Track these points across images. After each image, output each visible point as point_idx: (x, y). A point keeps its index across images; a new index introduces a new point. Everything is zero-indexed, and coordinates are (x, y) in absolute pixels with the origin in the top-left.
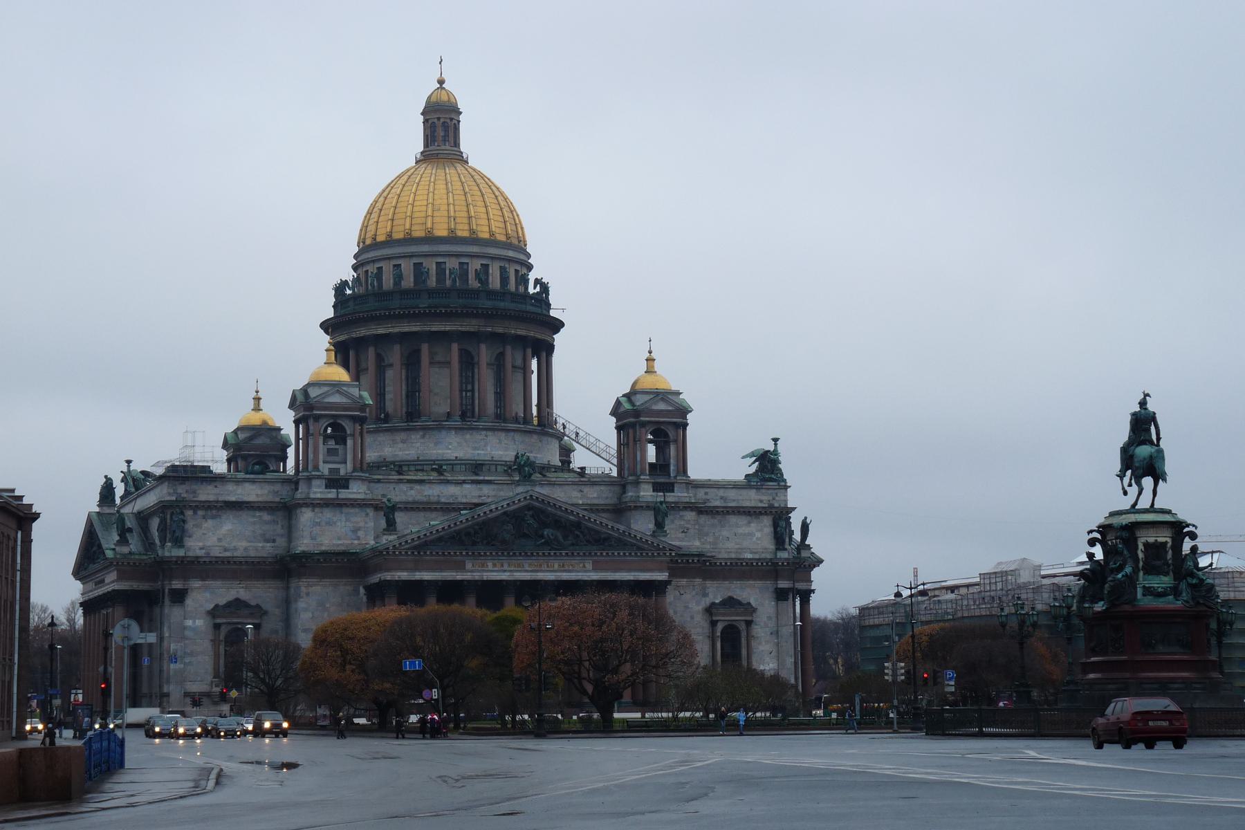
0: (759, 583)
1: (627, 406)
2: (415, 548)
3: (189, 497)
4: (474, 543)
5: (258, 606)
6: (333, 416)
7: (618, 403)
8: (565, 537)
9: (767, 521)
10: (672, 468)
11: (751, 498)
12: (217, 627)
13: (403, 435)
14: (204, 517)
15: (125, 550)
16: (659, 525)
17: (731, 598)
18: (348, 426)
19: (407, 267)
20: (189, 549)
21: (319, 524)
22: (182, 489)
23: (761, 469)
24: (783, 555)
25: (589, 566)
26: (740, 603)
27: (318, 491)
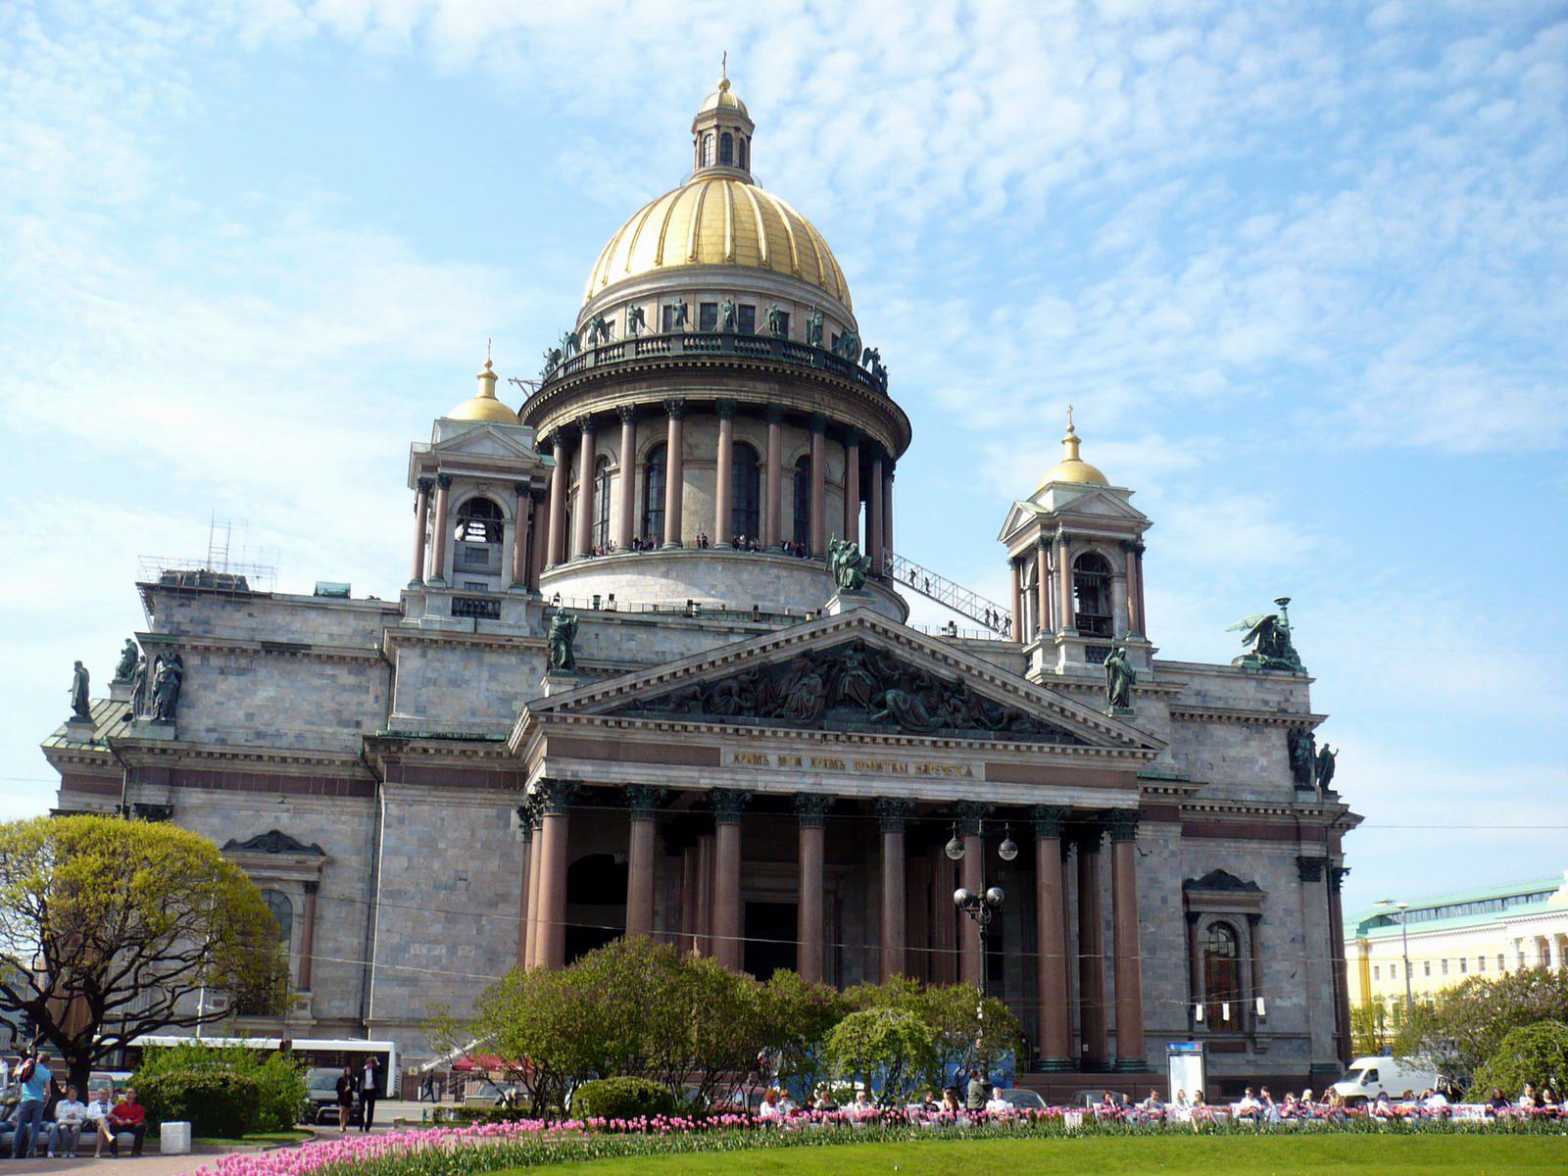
2: (611, 712)
3: (200, 630)
4: (739, 711)
5: (316, 850)
6: (479, 482)
8: (932, 710)
9: (1277, 739)
10: (1117, 624)
11: (1248, 696)
14: (222, 672)
15: (83, 734)
16: (1122, 701)
17: (1221, 873)
18: (510, 506)
19: (650, 311)
20: (185, 730)
21: (435, 683)
22: (182, 615)
25: (980, 772)
26: (1235, 884)
27: (433, 618)
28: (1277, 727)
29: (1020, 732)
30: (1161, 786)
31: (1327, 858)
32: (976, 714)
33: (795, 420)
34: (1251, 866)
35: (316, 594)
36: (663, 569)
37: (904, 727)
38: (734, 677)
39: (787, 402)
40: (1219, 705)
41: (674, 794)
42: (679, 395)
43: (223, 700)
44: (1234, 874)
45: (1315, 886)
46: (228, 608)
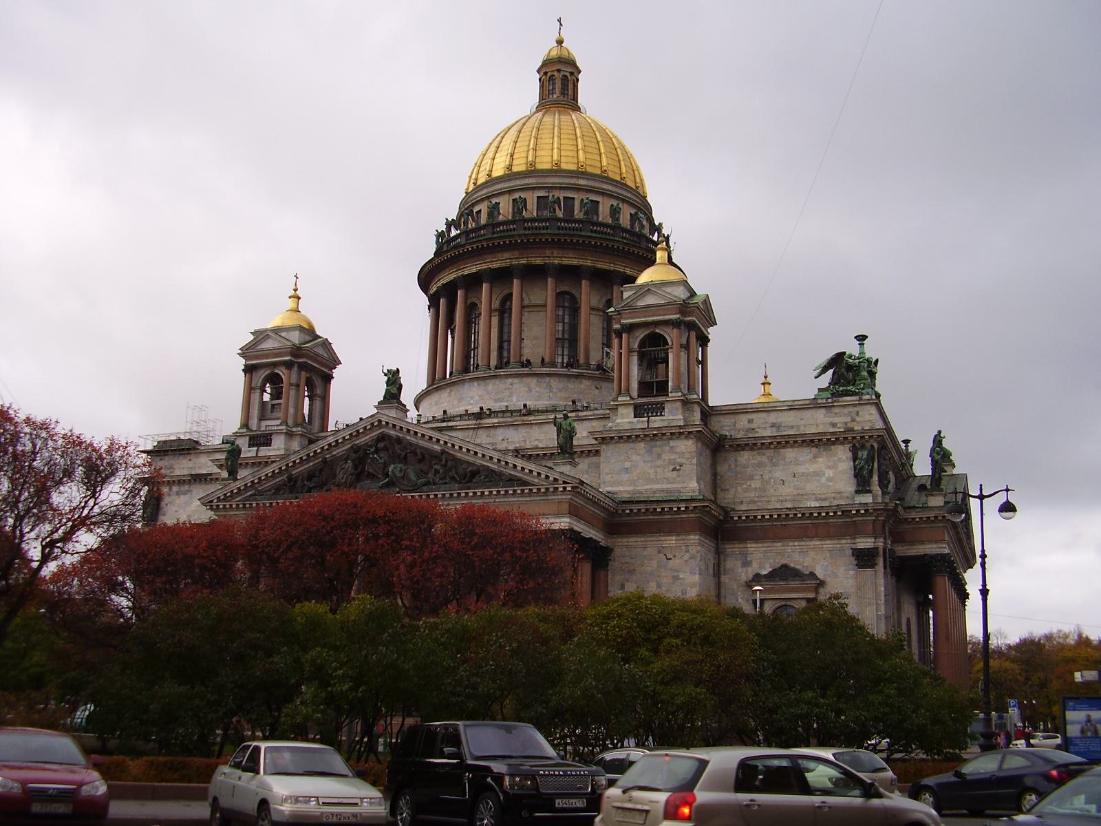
0: (828, 544)
9: (842, 455)
10: (670, 384)
11: (818, 422)
17: (785, 566)
23: (835, 381)
24: (867, 499)
28: (842, 443)
32: (453, 473)
34: (814, 559)
35: (223, 443)
36: (448, 391)
37: (400, 488)
39: (524, 261)
42: (460, 273)
43: (177, 509)
44: (798, 567)
45: (869, 571)
46: (181, 457)
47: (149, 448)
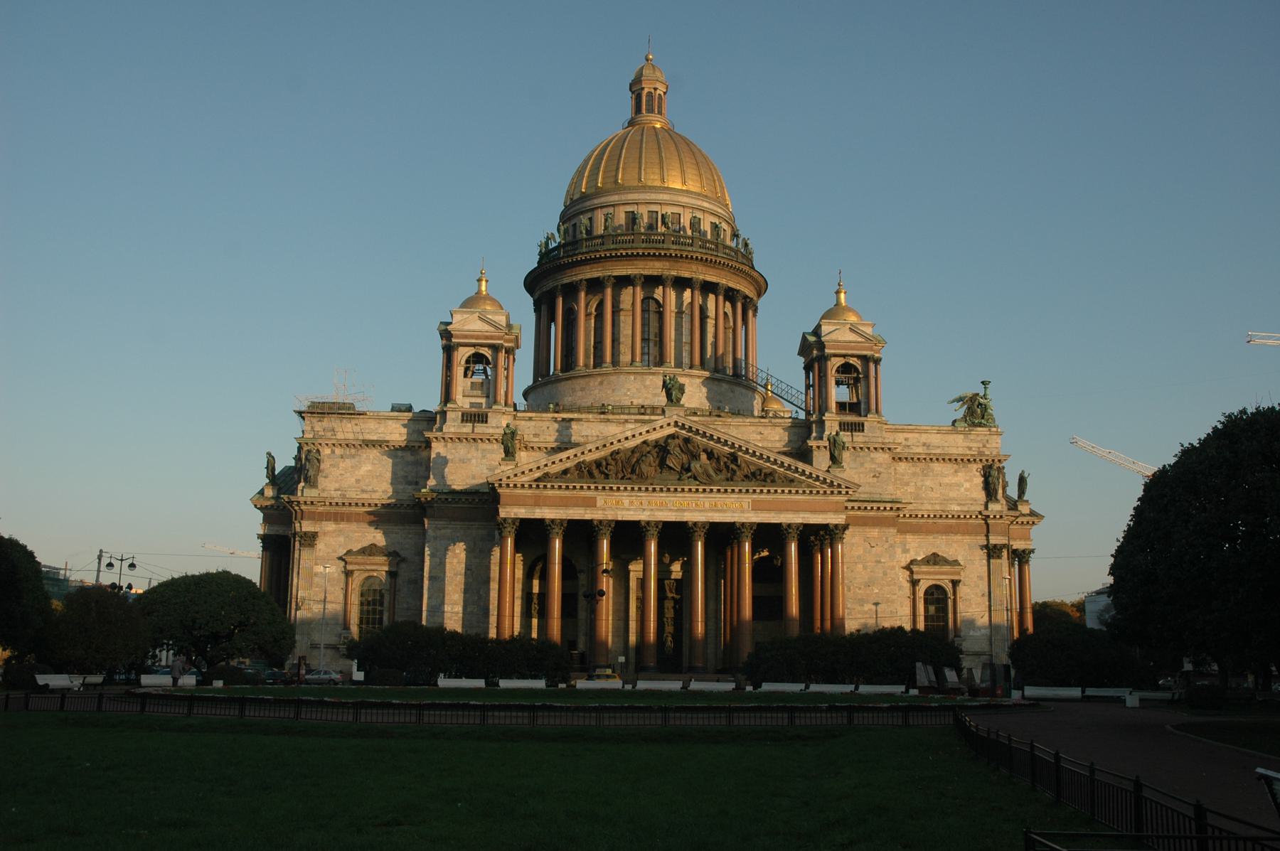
0: (967, 539)
1: (812, 339)
2: (536, 481)
3: (329, 434)
4: (607, 476)
6: (474, 345)
7: (804, 338)
8: (718, 470)
9: (975, 469)
11: (958, 444)
12: (348, 574)
13: (582, 382)
17: (934, 554)
20: (324, 490)
22: (320, 426)
26: (946, 562)
29: (773, 481)
30: (882, 506)
31: (1004, 546)
33: (681, 284)
35: (393, 410)
36: (599, 379)
38: (606, 459)
40: (938, 451)
41: (571, 522)
47: (303, 409)
